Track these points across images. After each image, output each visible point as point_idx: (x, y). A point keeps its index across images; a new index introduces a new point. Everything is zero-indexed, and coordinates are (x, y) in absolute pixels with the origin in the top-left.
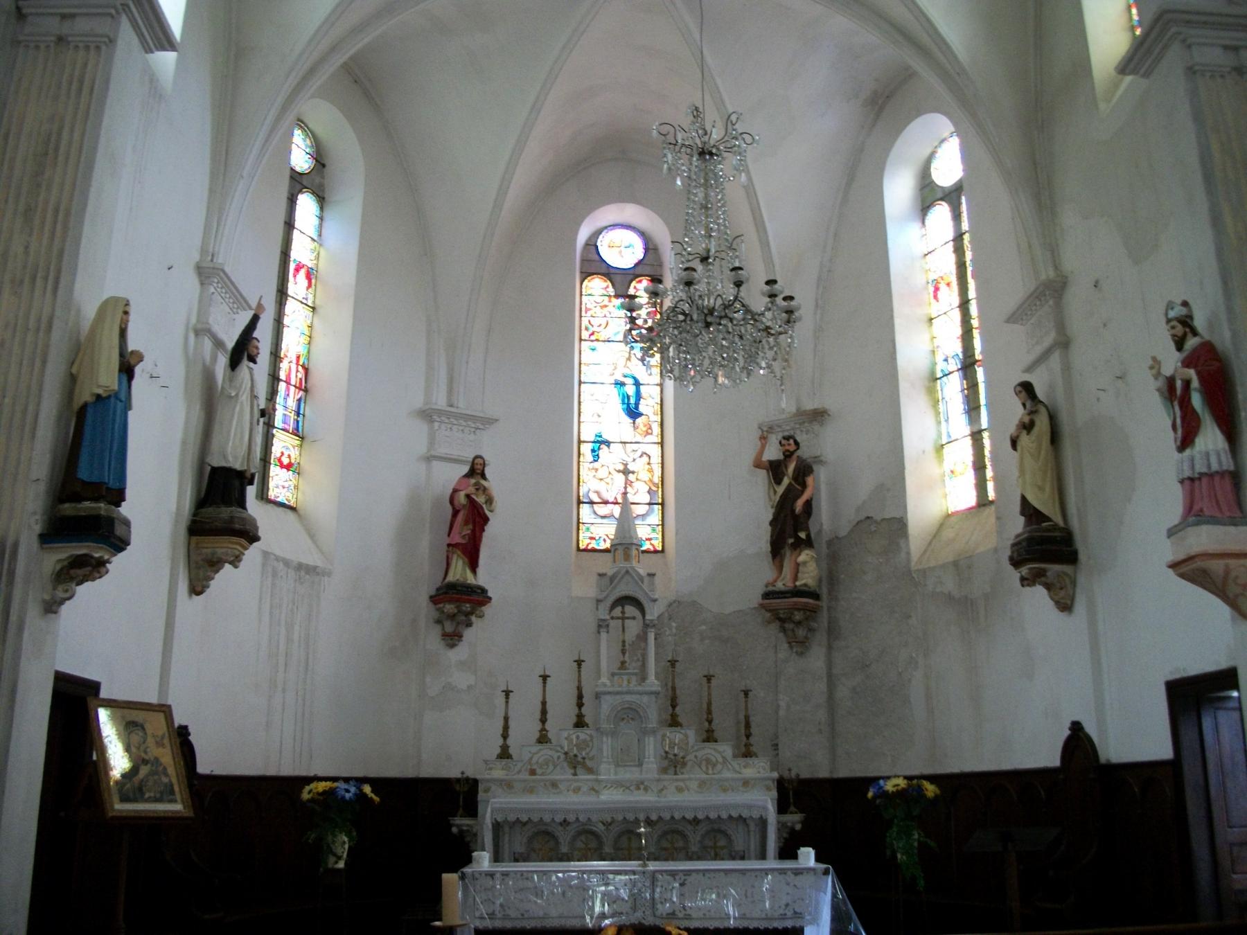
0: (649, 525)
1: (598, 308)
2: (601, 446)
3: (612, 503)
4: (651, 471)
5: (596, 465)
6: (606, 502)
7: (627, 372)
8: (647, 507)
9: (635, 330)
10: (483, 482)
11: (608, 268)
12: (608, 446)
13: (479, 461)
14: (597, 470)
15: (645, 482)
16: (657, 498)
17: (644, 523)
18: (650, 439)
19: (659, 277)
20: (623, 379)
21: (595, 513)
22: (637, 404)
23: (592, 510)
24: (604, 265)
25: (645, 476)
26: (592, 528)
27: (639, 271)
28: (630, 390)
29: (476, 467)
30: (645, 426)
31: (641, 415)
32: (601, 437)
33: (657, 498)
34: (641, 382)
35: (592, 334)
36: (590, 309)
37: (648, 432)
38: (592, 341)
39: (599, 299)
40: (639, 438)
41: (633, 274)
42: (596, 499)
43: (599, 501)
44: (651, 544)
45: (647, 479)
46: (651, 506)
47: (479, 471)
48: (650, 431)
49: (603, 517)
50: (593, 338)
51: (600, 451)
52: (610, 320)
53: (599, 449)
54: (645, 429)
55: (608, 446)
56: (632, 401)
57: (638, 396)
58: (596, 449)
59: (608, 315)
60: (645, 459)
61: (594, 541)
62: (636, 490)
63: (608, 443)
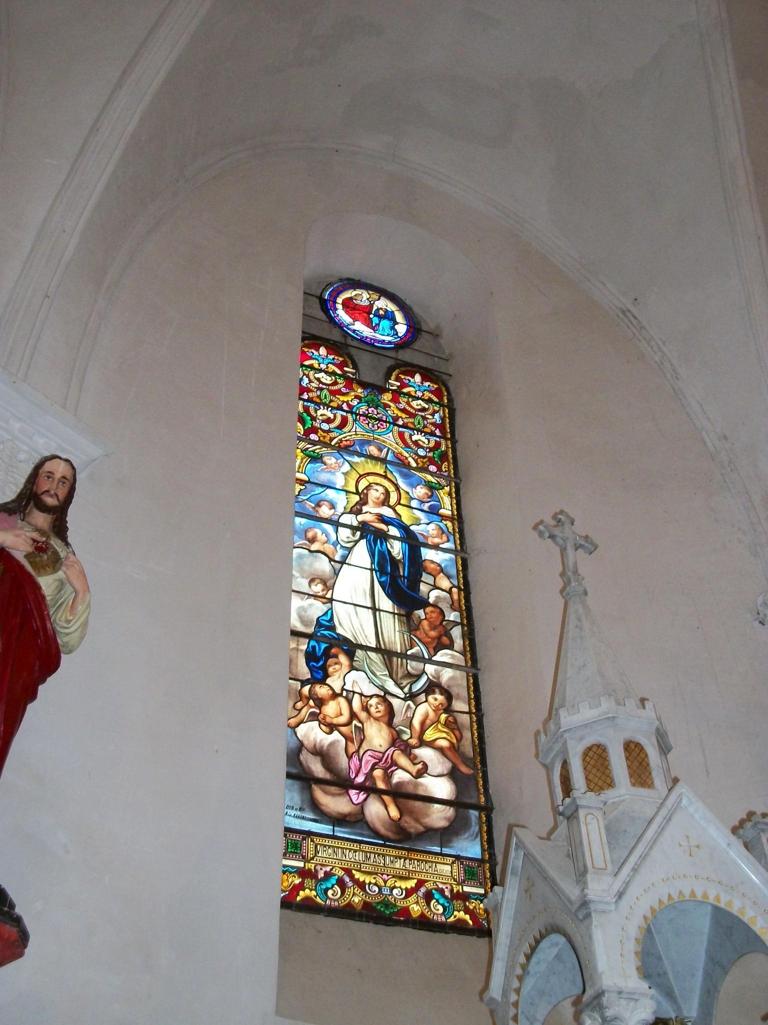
0: (458, 857)
1: (325, 392)
2: (333, 651)
3: (360, 788)
4: (452, 726)
5: (322, 691)
6: (343, 783)
7: (387, 512)
8: (450, 812)
9: (357, 503)
10: (56, 543)
11: (345, 337)
12: (351, 655)
13: (60, 469)
14: (320, 702)
15: (441, 750)
16: (474, 794)
17: (446, 851)
18: (443, 656)
19: (445, 377)
20: (383, 526)
21: (315, 806)
22: (415, 580)
23: (307, 796)
24: (337, 329)
25: (437, 735)
26: (309, 847)
27: (406, 355)
28: (397, 549)
29: (44, 485)
30: (433, 628)
31: (424, 603)
32: (332, 628)
33: (474, 794)
34: (421, 539)
35: (314, 430)
36: (308, 390)
37: (442, 642)
38: (314, 443)
39: (327, 379)
40: (419, 649)
41: (396, 359)
42: (317, 769)
43: (328, 776)
44: (467, 911)
45: (444, 743)
46: (461, 810)
47: (50, 501)
48: (445, 640)
49: (339, 820)
50: (313, 437)
51: (331, 661)
52: (350, 417)
53: (327, 654)
54: (433, 634)
55: (351, 655)
56: (404, 571)
57: (416, 564)
58: (319, 653)
59: (345, 407)
60: (438, 698)
61: (309, 882)
62: (420, 766)
63: (350, 648)
